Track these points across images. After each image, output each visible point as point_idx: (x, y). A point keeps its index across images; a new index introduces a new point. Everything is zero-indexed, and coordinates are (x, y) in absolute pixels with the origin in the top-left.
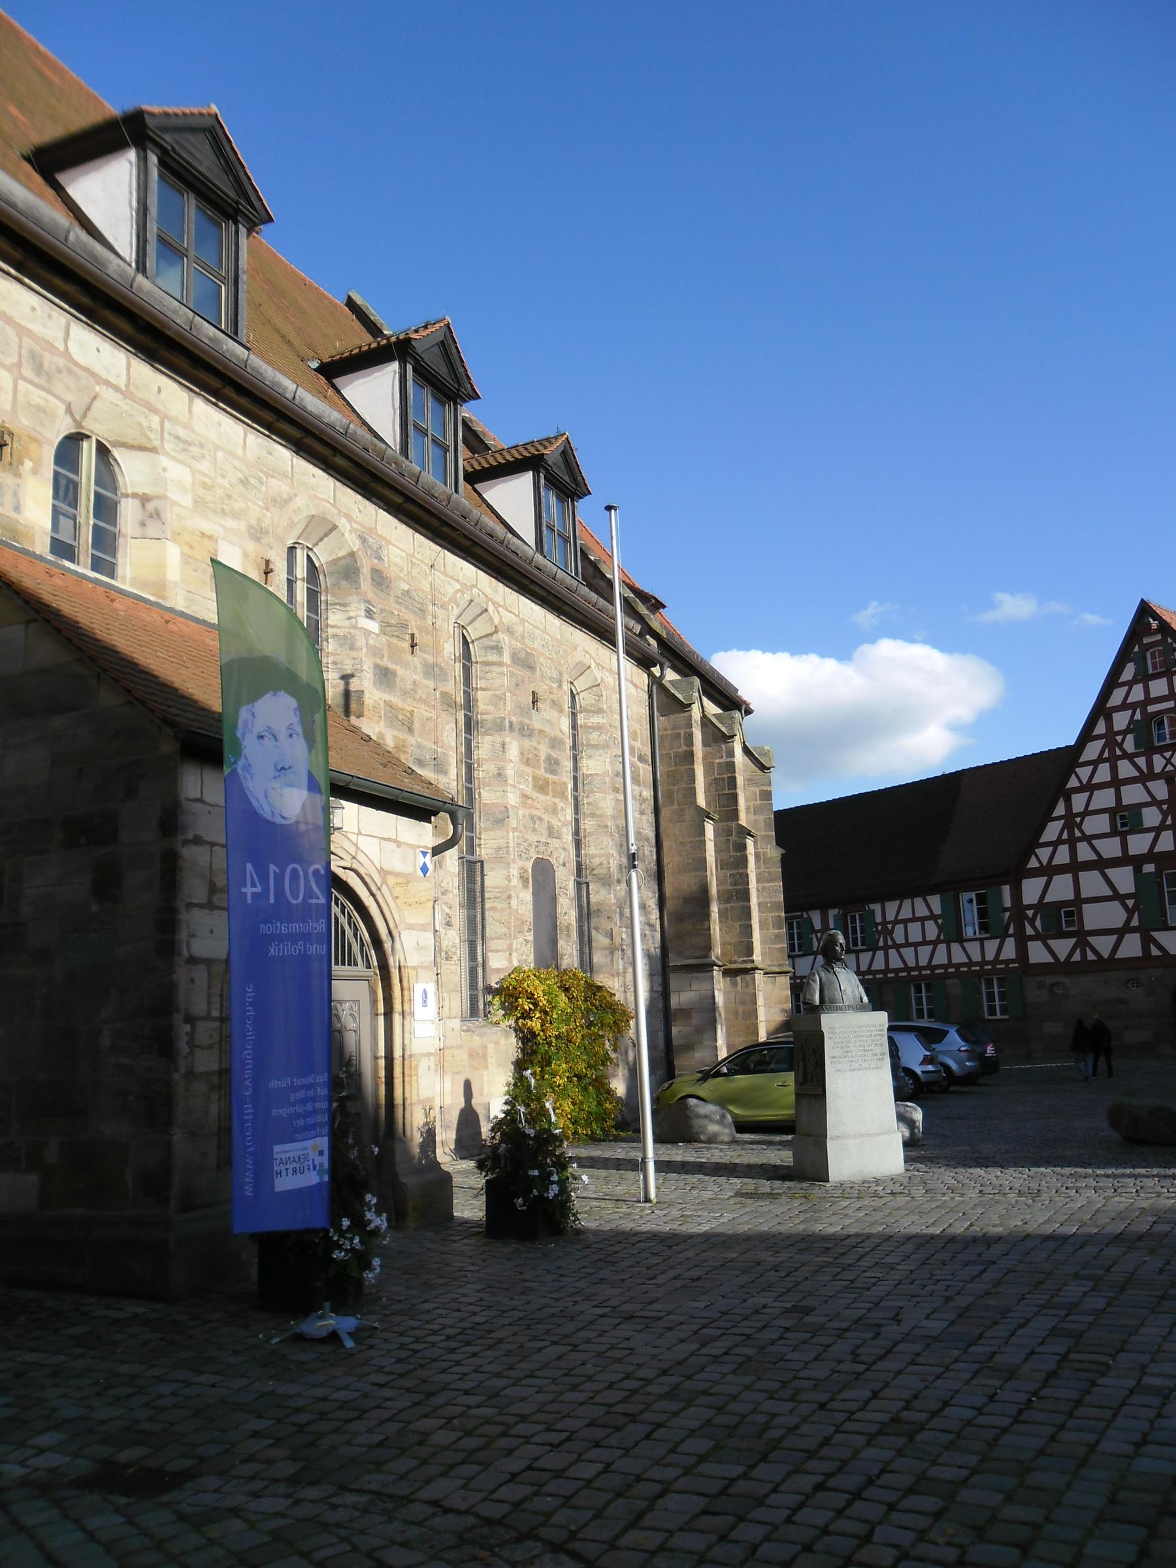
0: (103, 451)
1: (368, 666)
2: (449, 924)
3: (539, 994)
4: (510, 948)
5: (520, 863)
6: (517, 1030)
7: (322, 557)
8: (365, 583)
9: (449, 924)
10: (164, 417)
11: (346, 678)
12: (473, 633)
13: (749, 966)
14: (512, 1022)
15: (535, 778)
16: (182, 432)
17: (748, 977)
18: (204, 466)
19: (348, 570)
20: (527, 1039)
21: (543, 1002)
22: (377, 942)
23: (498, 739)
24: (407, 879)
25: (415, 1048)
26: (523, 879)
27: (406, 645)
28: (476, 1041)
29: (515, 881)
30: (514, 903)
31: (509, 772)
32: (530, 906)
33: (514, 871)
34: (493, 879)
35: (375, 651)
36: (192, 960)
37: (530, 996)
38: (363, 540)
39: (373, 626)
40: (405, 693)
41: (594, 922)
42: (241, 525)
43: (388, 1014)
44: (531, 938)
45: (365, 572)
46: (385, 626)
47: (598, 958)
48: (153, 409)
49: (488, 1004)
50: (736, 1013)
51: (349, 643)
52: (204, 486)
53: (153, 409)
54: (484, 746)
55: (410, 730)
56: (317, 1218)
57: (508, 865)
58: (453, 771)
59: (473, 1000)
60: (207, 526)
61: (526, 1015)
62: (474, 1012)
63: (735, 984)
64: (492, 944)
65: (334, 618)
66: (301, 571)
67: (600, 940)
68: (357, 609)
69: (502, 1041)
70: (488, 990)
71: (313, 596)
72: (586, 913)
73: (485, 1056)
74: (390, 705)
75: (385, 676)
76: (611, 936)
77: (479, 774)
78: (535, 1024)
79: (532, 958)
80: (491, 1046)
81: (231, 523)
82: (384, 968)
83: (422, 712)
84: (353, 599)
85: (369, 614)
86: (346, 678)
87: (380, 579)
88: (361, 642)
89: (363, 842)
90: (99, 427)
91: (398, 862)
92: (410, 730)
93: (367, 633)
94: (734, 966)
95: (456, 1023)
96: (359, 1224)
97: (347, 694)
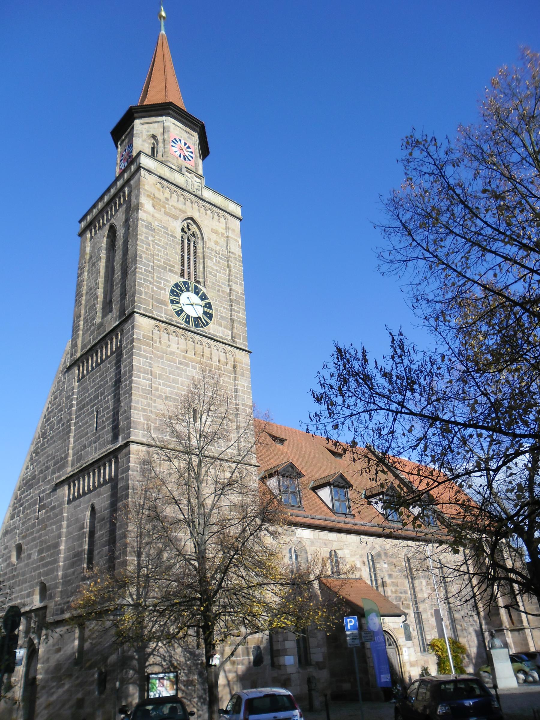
0: (335, 551)
1: (386, 575)
2: (414, 630)
3: (439, 645)
4: (431, 634)
5: (431, 611)
6: (436, 655)
7: (373, 553)
8: (383, 557)
9: (414, 630)
10: (343, 542)
11: (382, 579)
12: (409, 556)
13: (522, 627)
14: (434, 653)
15: (431, 588)
16: (346, 543)
17: (523, 631)
18: (351, 548)
19: (379, 555)
20: (439, 657)
21: (441, 647)
22: (395, 642)
23: (420, 581)
24: (398, 629)
25: (405, 661)
26: (432, 615)
27: (394, 567)
28: (425, 658)
29: (430, 616)
30: (430, 622)
31: (424, 588)
32: (435, 622)
33: (429, 614)
34: (424, 616)
35: (387, 571)
36: (368, 649)
37: (437, 646)
38: (381, 547)
39: (386, 565)
40: (395, 578)
41: (456, 622)
42: (358, 556)
43: (399, 655)
44: (436, 630)
45: (383, 554)
46: (389, 564)
47: (459, 633)
48: (341, 542)
49: (428, 648)
50: (522, 644)
51: (381, 571)
52: (351, 552)
53: (341, 542)
54: (417, 583)
55: (398, 586)
56: (390, 685)
57: (427, 612)
58: (409, 593)
59: (424, 647)
60: (353, 559)
61: (437, 651)
62: (425, 651)
63: (519, 634)
64: (427, 633)
65: (378, 565)
66: (370, 558)
67: (458, 627)
68: (382, 563)
69: (432, 658)
70: (427, 645)
71: (373, 562)
72: (453, 621)
73: (428, 662)
74: (392, 582)
75: (390, 576)
76: (461, 626)
77: (416, 590)
78: (440, 653)
79: (437, 635)
80: (429, 660)
81: (357, 557)
82: (397, 646)
83: (399, 581)
84: (381, 561)
85: (385, 563)
86: (382, 579)
87: (386, 554)
88: (384, 570)
89: (389, 624)
90: (334, 548)
91: (396, 626)
92: (398, 586)
93: (385, 567)
94: (518, 628)
95: (420, 654)
96: (396, 688)
97: (383, 582)
